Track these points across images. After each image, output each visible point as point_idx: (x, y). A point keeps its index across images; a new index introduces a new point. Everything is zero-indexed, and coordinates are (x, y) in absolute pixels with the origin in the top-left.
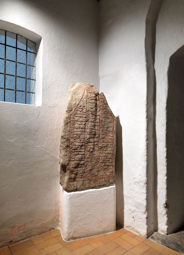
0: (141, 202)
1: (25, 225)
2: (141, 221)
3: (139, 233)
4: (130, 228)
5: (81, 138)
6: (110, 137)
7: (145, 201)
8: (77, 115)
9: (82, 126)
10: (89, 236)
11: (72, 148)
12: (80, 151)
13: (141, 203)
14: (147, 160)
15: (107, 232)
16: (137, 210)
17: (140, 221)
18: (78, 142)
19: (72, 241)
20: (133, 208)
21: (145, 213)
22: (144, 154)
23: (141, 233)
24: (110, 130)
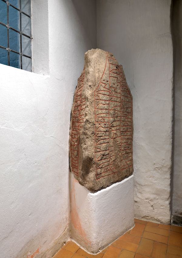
0: (164, 188)
1: (38, 251)
2: (162, 208)
3: (159, 221)
4: (148, 218)
5: (105, 122)
6: (129, 119)
8: (100, 92)
9: (106, 106)
10: (115, 239)
11: (98, 135)
12: (105, 139)
13: (164, 190)
14: (172, 143)
15: (129, 229)
16: (157, 198)
17: (161, 208)
18: (103, 126)
19: (101, 252)
20: (152, 196)
21: (168, 199)
23: (163, 221)
24: (129, 111)
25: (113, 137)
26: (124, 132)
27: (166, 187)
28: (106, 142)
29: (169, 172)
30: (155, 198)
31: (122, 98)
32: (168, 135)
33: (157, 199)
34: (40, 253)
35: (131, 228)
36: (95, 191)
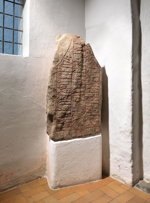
0: (127, 151)
1: (12, 174)
2: (127, 170)
3: (124, 181)
4: (116, 176)
5: (67, 89)
6: (96, 87)
7: (131, 150)
8: (63, 66)
9: (68, 76)
10: (76, 185)
11: (59, 98)
12: (67, 101)
13: (127, 152)
14: (132, 110)
15: (93, 181)
16: (123, 159)
17: (125, 170)
18: (65, 92)
19: (58, 189)
20: (119, 157)
21: (131, 162)
22: (130, 104)
23: (126, 182)
24: (96, 80)
25: (76, 100)
26: (90, 98)
27: (128, 150)
28: (67, 104)
29: (131, 136)
30: (121, 159)
31: (87, 70)
32: (129, 103)
33: (123, 160)
34: (14, 176)
35: (95, 180)
36: (55, 140)
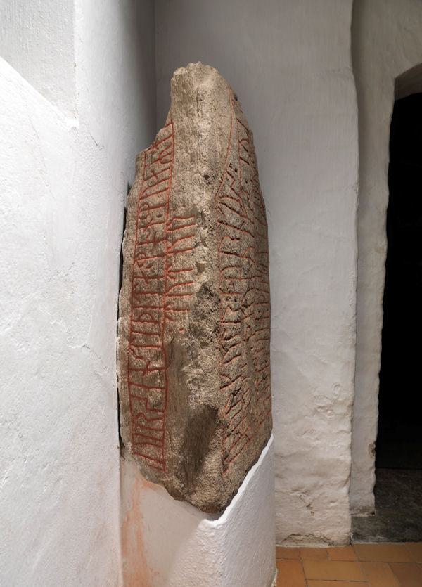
0: (337, 457)
3: (324, 540)
7: (348, 452)
16: (321, 483)
22: (351, 328)
32: (348, 325)
33: (322, 486)
